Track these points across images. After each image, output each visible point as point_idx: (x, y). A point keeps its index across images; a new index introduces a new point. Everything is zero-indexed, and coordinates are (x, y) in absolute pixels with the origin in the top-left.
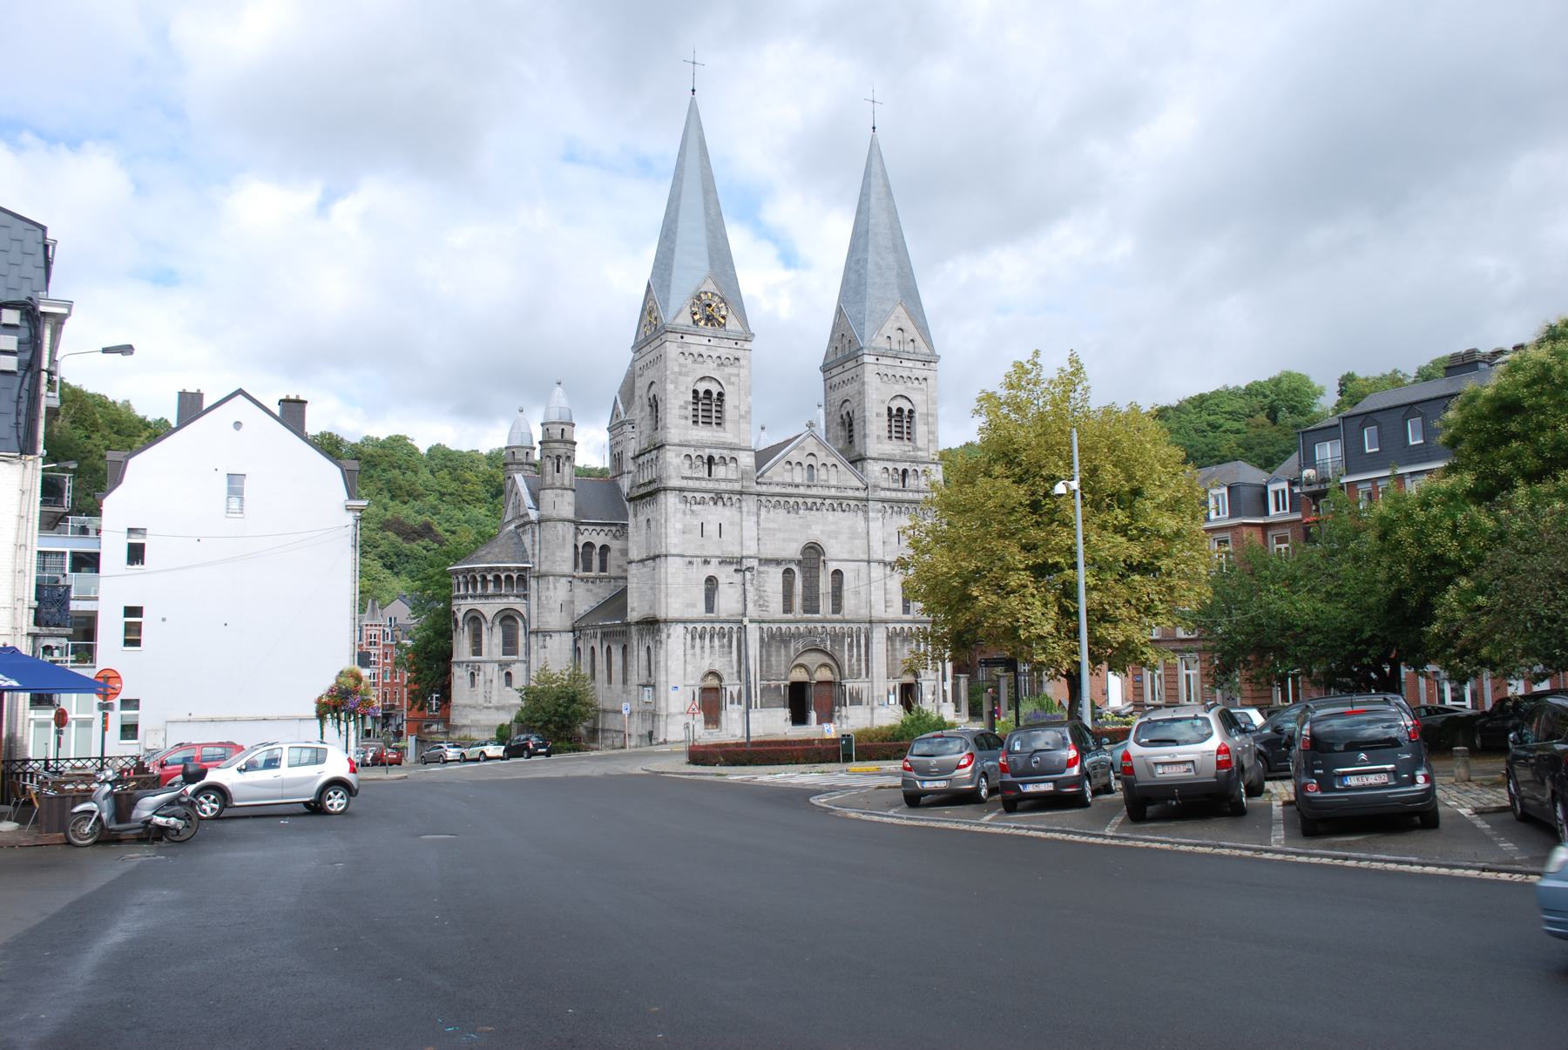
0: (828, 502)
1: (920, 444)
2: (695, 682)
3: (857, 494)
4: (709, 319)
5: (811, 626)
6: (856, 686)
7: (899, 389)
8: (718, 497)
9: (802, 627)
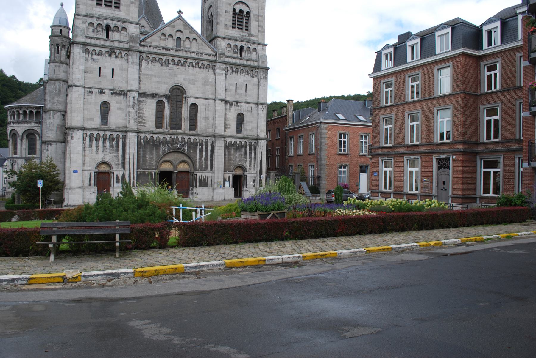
0: (189, 61)
2: (91, 167)
3: (210, 58)
5: (174, 137)
6: (204, 175)
8: (111, 52)
9: (168, 137)
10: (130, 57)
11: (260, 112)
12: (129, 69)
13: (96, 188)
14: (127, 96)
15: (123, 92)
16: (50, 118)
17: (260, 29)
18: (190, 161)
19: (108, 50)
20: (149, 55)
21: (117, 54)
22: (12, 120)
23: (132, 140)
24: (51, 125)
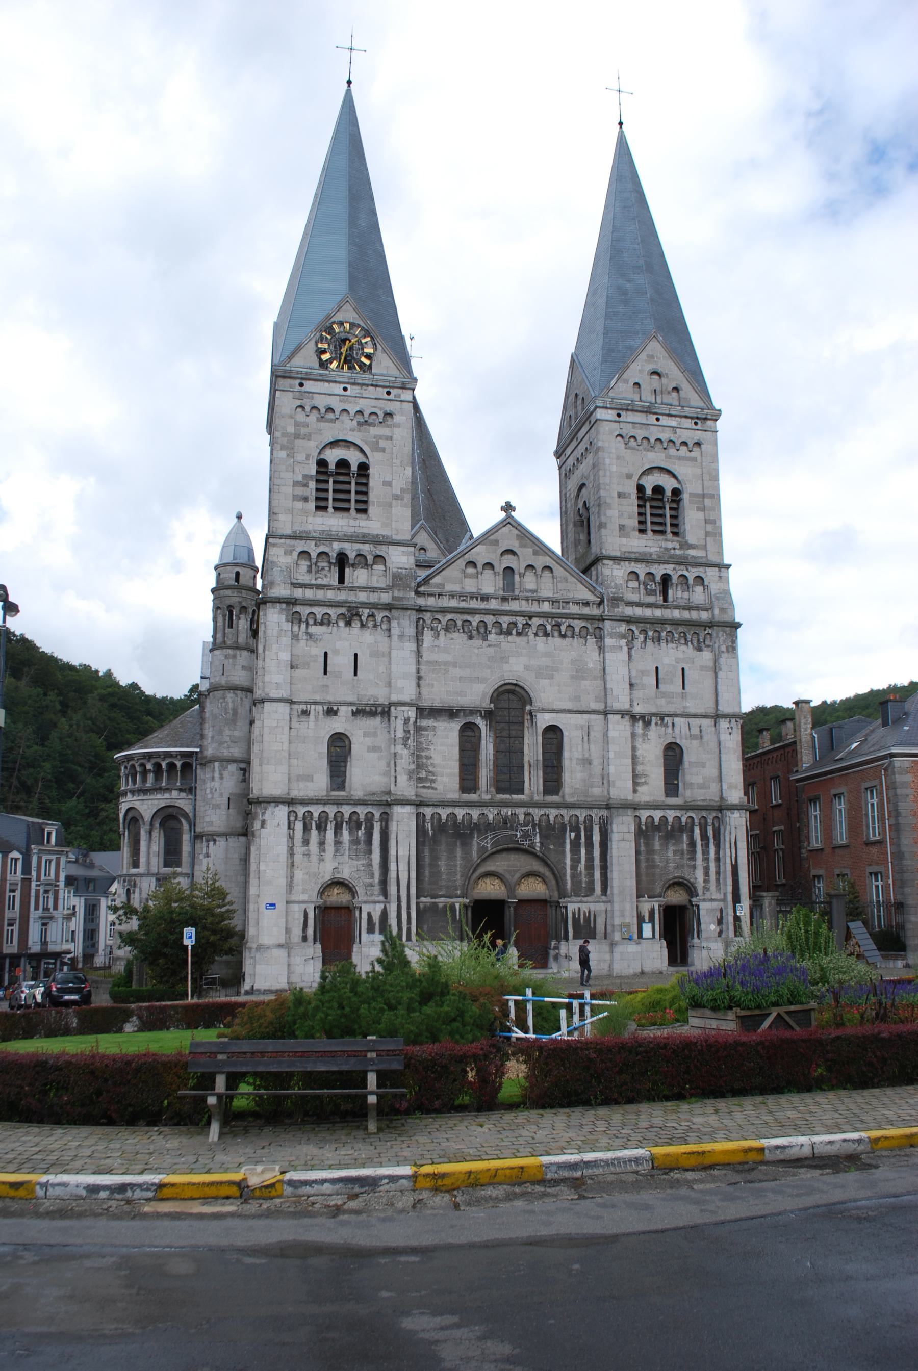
0: (536, 622)
1: (691, 538)
2: (307, 895)
3: (586, 611)
4: (349, 361)
6: (585, 908)
7: (656, 458)
8: (351, 615)
9: (491, 814)
10: (394, 624)
11: (724, 737)
12: (394, 653)
13: (319, 946)
14: (389, 716)
15: (380, 709)
16: (213, 779)
17: (709, 528)
18: (548, 874)
19: (343, 610)
20: (439, 616)
21: (364, 618)
22: (130, 786)
23: (404, 822)
24: (216, 795)
